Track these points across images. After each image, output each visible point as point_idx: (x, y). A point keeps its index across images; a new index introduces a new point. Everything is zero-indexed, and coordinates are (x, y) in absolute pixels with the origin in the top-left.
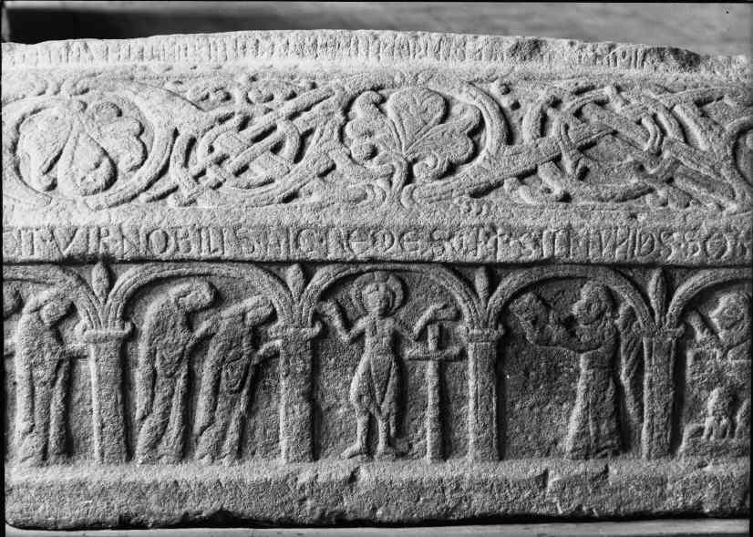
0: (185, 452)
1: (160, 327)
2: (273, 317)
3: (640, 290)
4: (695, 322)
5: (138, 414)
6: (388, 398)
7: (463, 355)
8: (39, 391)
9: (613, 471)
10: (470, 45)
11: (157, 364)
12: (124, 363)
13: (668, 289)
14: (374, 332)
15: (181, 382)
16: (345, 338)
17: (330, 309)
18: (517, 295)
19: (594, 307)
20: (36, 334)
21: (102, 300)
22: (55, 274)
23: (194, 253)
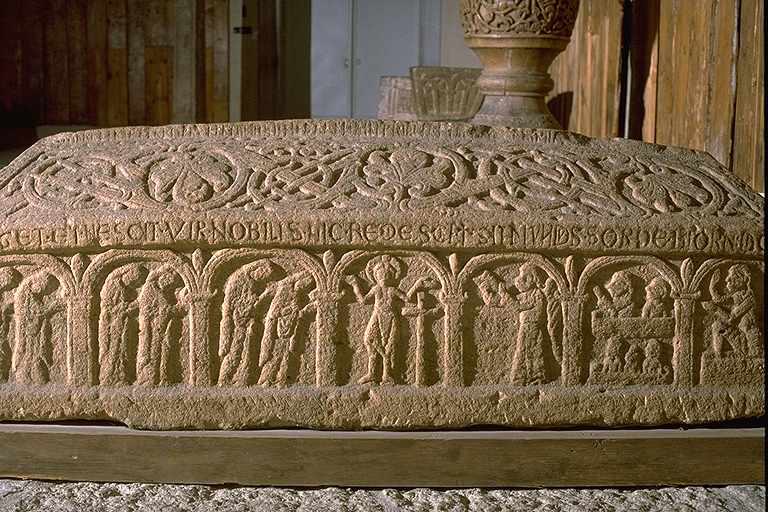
0: (252, 379)
1: (236, 291)
2: (313, 286)
3: (560, 268)
4: (596, 290)
5: (220, 353)
7: (441, 313)
8: (156, 336)
9: (542, 393)
10: (442, 128)
12: (213, 316)
13: (578, 268)
14: (381, 296)
16: (361, 300)
17: (351, 280)
18: (478, 272)
19: (529, 279)
20: (151, 295)
21: (198, 273)
23: (261, 239)
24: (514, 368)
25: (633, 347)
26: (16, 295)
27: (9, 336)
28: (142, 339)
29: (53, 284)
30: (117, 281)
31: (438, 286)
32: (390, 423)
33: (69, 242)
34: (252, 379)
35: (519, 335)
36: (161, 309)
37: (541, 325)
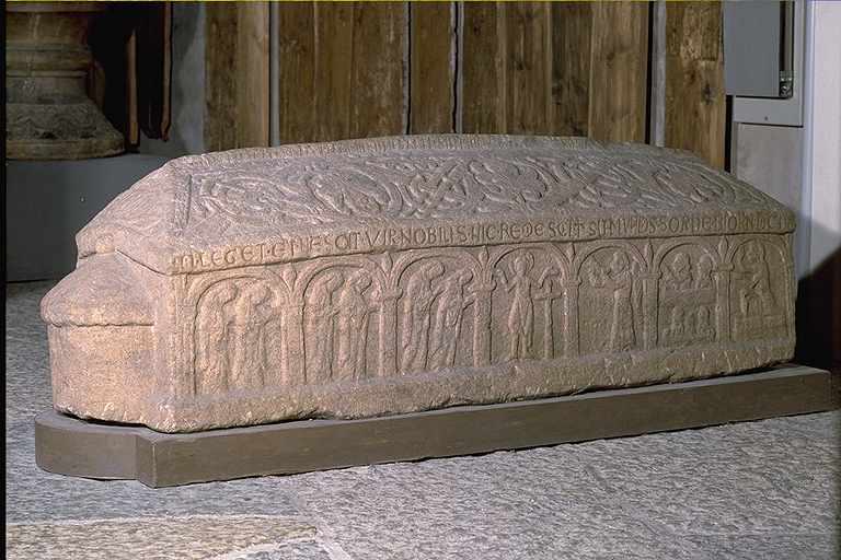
0: (425, 368)
6: (528, 323)
9: (633, 357)
11: (415, 312)
12: (397, 313)
15: (426, 322)
22: (361, 260)
24: (613, 337)
25: (690, 314)
26: (237, 308)
27: (230, 346)
28: (343, 340)
29: (269, 295)
30: (323, 286)
31: (559, 274)
32: (533, 393)
33: (287, 255)
34: (425, 368)
35: (615, 311)
36: (359, 309)
37: (630, 299)
